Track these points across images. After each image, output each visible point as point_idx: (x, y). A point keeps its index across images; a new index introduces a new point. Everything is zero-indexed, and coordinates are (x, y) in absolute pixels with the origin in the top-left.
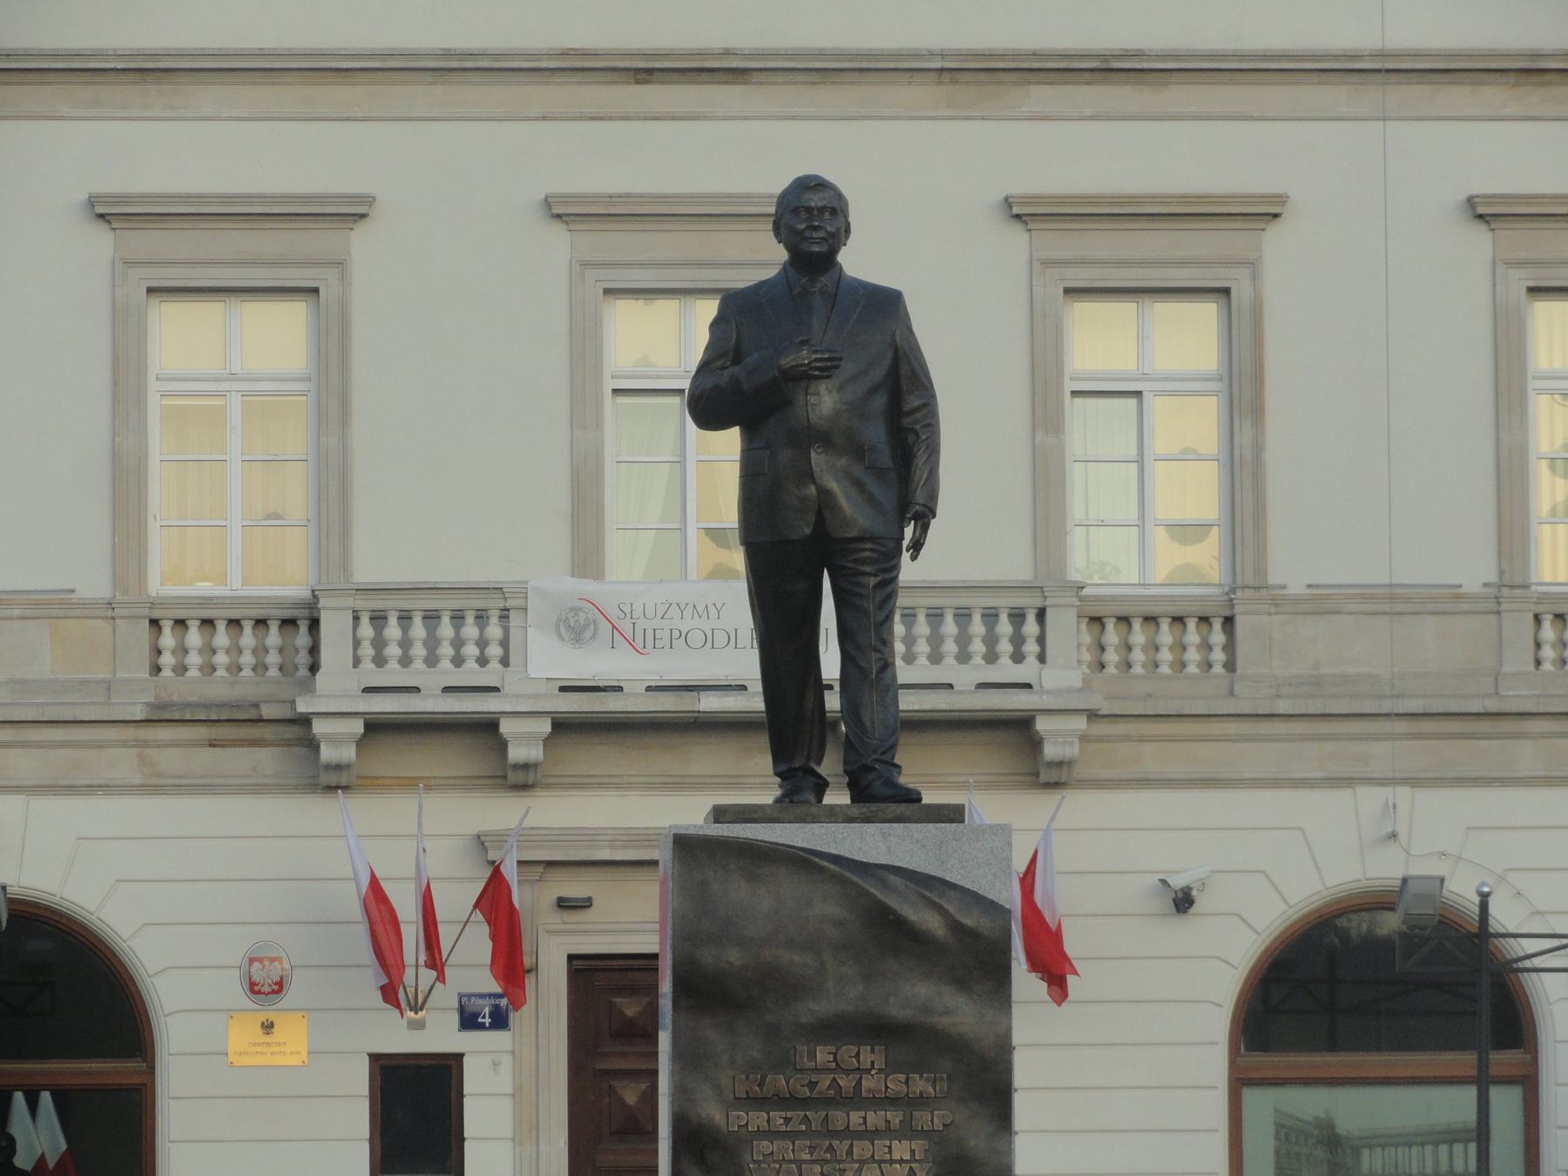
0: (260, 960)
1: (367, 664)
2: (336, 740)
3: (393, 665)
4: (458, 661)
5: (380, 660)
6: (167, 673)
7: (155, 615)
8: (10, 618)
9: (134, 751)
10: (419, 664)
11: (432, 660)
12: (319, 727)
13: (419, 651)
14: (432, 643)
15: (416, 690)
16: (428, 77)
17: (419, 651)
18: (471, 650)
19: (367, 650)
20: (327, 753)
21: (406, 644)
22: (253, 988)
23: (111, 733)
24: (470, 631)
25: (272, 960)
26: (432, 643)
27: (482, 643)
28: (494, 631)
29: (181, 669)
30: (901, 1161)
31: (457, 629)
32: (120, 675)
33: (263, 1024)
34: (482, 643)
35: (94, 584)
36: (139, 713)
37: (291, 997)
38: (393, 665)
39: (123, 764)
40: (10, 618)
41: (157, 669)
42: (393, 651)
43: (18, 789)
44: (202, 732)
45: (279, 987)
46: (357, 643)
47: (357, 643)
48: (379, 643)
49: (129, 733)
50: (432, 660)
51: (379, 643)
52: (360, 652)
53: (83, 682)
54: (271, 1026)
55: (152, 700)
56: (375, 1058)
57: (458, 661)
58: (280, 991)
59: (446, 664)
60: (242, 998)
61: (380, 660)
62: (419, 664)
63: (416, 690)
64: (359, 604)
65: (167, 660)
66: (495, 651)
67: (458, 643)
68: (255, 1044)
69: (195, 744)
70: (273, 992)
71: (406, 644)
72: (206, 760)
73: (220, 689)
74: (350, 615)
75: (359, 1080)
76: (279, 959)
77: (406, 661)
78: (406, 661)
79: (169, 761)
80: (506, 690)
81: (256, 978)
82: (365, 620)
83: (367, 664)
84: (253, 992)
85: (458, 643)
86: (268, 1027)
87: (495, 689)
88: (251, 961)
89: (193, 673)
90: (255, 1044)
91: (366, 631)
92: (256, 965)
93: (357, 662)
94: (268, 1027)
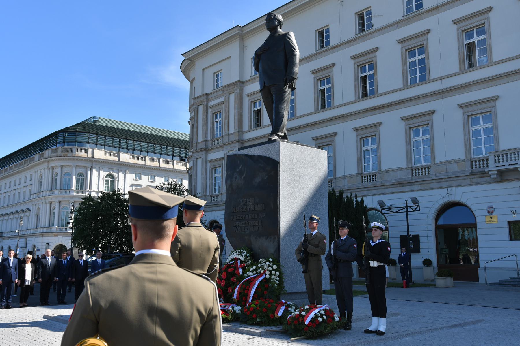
0: (489, 208)
1: (497, 163)
2: (493, 174)
3: (501, 162)
4: (511, 160)
5: (499, 162)
6: (474, 168)
7: (472, 160)
8: (452, 163)
9: (469, 180)
10: (505, 162)
11: (507, 161)
12: (490, 173)
13: (505, 160)
14: (507, 158)
15: (504, 165)
16: (505, 77)
17: (505, 160)
18: (513, 159)
19: (497, 161)
20: (491, 176)
21: (503, 159)
22: (489, 212)
23: (465, 177)
24: (513, 156)
25: (491, 208)
26: (507, 158)
27: (515, 157)
28: (516, 155)
29: (476, 168)
30: (257, 226)
31: (511, 155)
32: (466, 169)
33: (490, 217)
34: (515, 157)
35: (463, 157)
36: (468, 174)
37: (495, 213)
38: (501, 162)
39: (468, 182)
40: (452, 163)
41: (472, 168)
42: (501, 160)
43: (454, 187)
44: (478, 176)
45: (493, 212)
46: (496, 160)
47: (496, 160)
48: (499, 159)
49: (468, 177)
50: (507, 161)
51: (499, 159)
52: (496, 161)
53: (462, 171)
54: (492, 217)
55: (471, 172)
56: (509, 222)
57: (511, 160)
58: (493, 212)
59: (509, 161)
60: (487, 214)
61: (499, 162)
62: (505, 162)
63: (504, 165)
64: (495, 154)
65: (474, 167)
66: (517, 158)
67: (511, 158)
68: (489, 220)
69: (478, 178)
70: (492, 212)
71: (503, 159)
72: (479, 180)
73: (480, 170)
74: (493, 156)
75: (506, 225)
76: (492, 208)
77: (503, 162)
78: (503, 162)
79: (475, 180)
80: (518, 164)
81: (489, 210)
82: (496, 156)
83: (497, 163)
84: (489, 213)
85: (511, 158)
86: (491, 218)
87: (517, 164)
88: (488, 208)
89: (478, 168)
90: (489, 220)
91: (497, 158)
92: (489, 209)
93: (496, 162)
94: (491, 218)
